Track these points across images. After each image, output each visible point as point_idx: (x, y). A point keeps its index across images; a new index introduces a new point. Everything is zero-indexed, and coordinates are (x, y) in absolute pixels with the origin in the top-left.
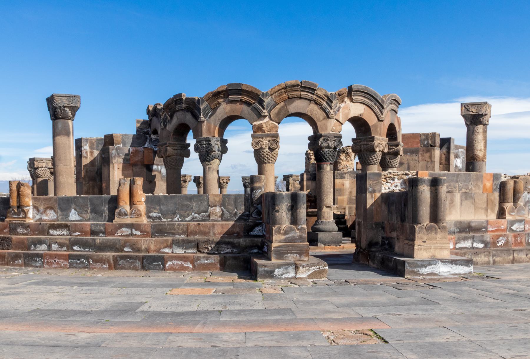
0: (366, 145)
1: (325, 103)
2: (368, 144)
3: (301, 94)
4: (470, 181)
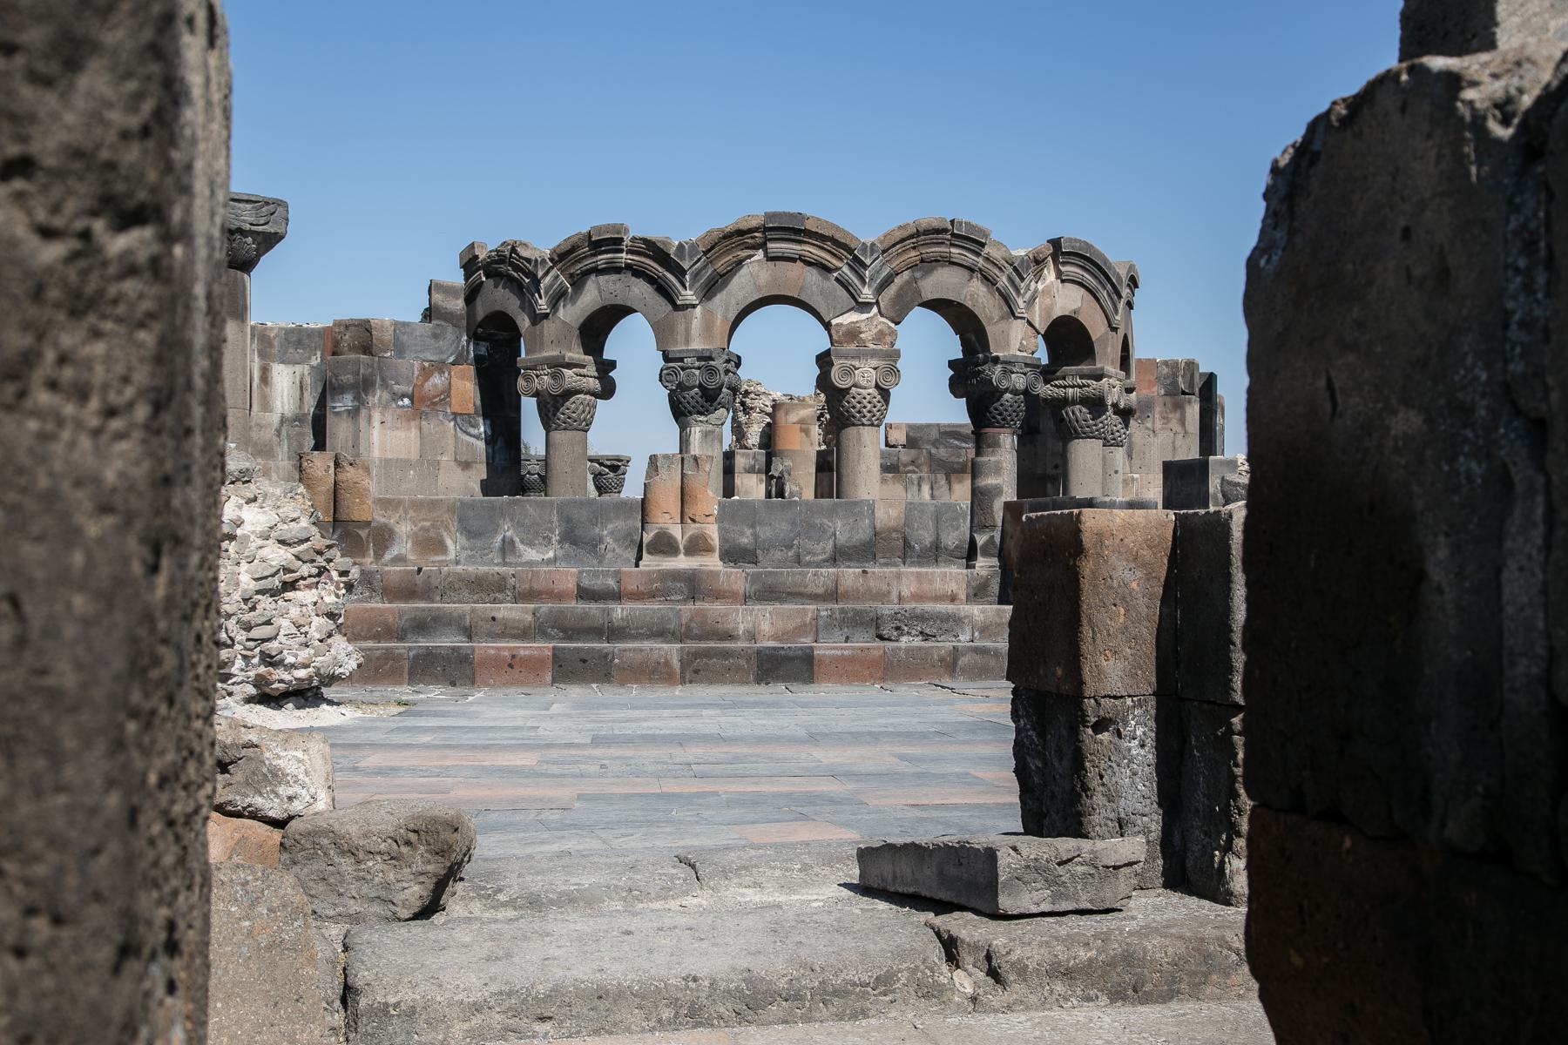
1: (1004, 279)
2: (1084, 386)
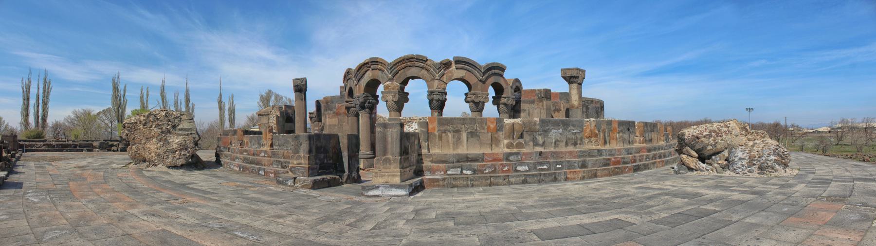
0: (471, 97)
1: (432, 70)
4: (476, 123)
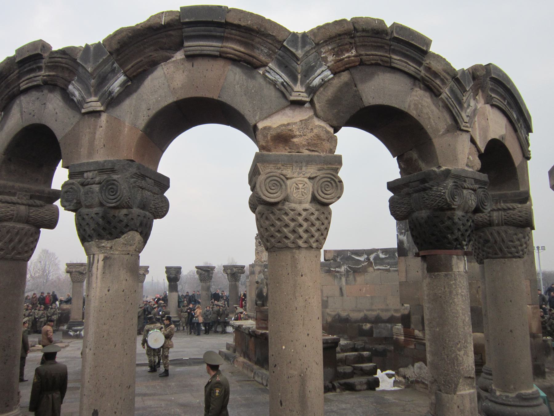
0: (504, 210)
2: (510, 209)
3: (391, 58)
